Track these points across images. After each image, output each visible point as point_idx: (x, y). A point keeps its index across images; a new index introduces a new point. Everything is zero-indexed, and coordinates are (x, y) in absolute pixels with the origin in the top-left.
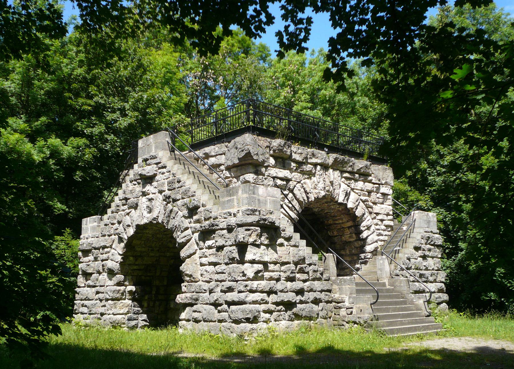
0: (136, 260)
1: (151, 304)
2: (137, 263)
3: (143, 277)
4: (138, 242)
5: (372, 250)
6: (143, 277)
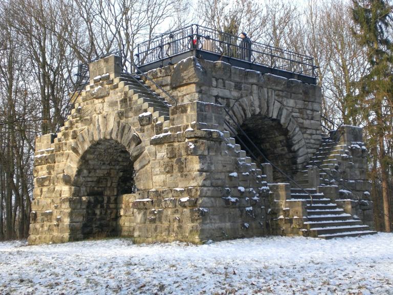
0: (89, 173)
1: (104, 212)
2: (90, 175)
3: (96, 188)
4: (92, 156)
5: (302, 162)
6: (96, 188)
